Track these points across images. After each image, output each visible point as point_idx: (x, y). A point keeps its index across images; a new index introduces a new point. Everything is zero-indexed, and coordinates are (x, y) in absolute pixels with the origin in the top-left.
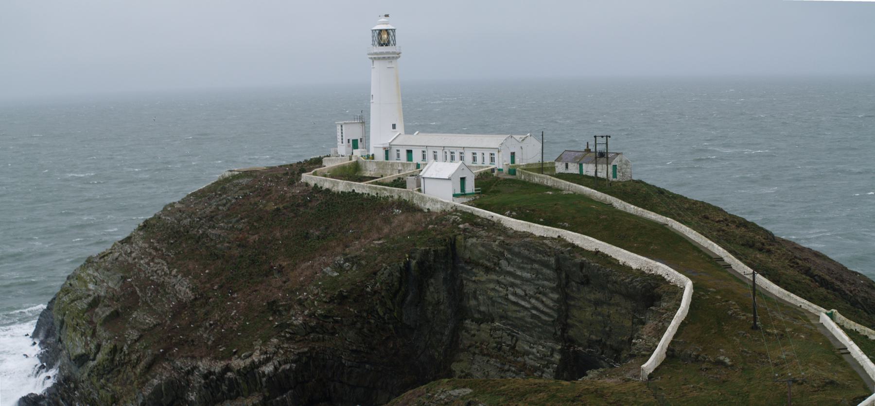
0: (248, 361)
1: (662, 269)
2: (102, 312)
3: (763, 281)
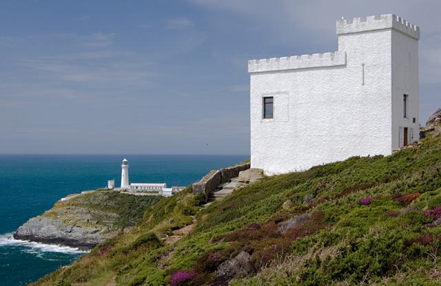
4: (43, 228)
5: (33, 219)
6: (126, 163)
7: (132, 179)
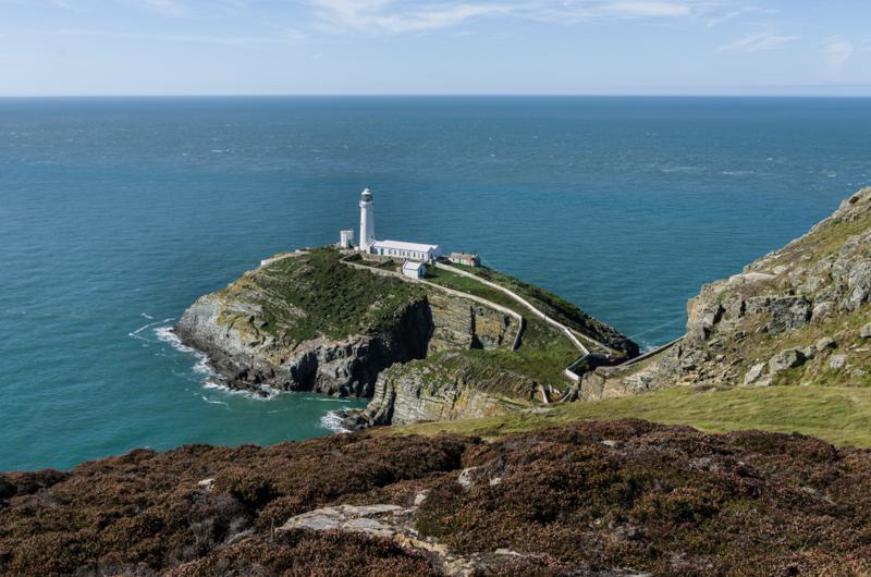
1: (509, 311)
2: (258, 323)
3: (548, 319)
5: (204, 298)
7: (380, 232)
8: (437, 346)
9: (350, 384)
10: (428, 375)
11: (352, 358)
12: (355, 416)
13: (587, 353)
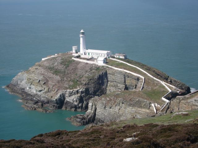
0: (77, 89)
2: (42, 83)
4: (23, 82)
5: (20, 74)
6: (83, 33)
7: (87, 47)
8: (110, 89)
9: (78, 105)
10: (108, 101)
11: (79, 95)
12: (81, 117)
13: (170, 91)
